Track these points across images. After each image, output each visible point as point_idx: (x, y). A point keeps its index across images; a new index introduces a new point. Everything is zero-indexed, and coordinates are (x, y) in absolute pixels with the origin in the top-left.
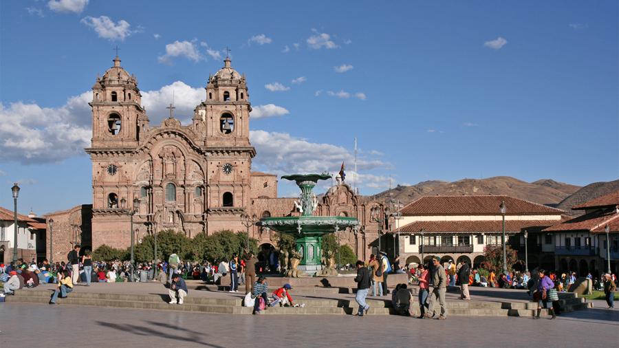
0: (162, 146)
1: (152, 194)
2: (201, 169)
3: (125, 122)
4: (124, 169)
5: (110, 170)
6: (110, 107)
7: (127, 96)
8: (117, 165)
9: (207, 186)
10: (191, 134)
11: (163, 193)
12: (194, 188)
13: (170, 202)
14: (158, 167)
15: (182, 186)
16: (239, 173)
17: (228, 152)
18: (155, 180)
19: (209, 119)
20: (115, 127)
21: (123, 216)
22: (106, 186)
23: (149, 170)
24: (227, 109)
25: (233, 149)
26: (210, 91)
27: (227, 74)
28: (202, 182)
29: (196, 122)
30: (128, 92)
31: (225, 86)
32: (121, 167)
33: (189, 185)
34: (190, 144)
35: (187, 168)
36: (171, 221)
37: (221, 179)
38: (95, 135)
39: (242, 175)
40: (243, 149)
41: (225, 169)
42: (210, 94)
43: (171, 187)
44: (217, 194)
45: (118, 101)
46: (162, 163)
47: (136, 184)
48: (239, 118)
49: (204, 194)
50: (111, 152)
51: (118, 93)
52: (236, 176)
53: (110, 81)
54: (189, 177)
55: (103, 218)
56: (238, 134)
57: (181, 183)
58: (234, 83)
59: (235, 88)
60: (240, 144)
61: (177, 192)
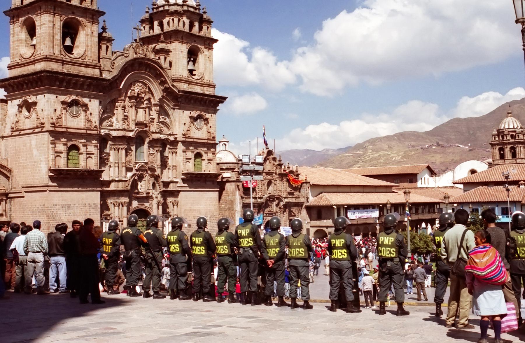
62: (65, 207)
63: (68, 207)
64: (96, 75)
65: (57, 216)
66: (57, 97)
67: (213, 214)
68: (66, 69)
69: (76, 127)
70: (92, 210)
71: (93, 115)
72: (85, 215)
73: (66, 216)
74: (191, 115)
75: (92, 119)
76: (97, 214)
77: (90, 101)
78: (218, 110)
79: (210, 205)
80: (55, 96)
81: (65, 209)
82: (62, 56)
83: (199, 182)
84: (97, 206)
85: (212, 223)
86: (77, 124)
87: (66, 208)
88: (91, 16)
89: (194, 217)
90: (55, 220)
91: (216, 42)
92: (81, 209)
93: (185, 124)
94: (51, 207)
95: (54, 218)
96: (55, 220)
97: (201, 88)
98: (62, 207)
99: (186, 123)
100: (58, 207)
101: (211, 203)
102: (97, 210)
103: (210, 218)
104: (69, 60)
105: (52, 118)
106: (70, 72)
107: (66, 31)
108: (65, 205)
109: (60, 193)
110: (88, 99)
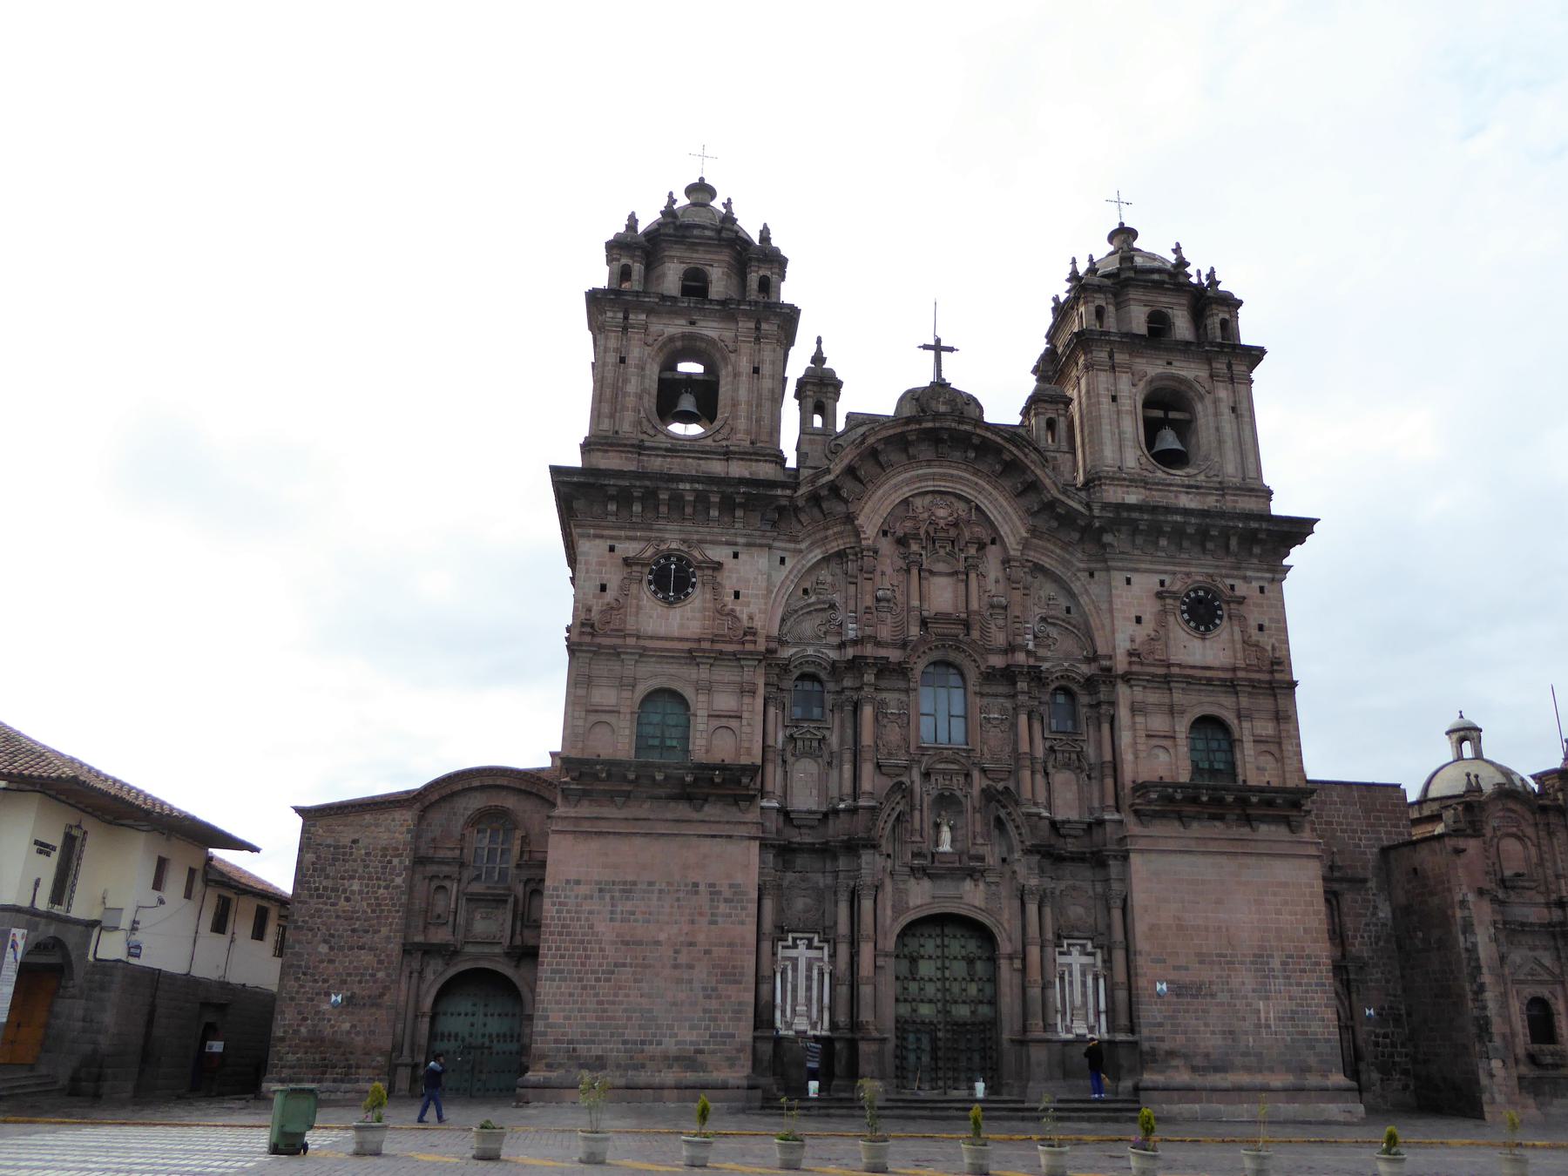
0: (906, 492)
3: (744, 378)
4: (729, 582)
6: (683, 322)
16: (1254, 632)
21: (712, 811)
22: (643, 654)
24: (1173, 370)
32: (718, 566)
36: (946, 847)
38: (606, 425)
39: (1266, 640)
44: (1159, 723)
48: (1226, 411)
50: (677, 501)
52: (1239, 646)
55: (608, 811)
56: (1230, 468)
62: (610, 891)
63: (624, 891)
65: (579, 919)
66: (612, 549)
67: (1303, 949)
70: (723, 908)
72: (693, 922)
73: (612, 920)
75: (738, 609)
76: (743, 923)
77: (736, 556)
78: (1289, 568)
79: (1278, 912)
80: (605, 544)
81: (612, 898)
82: (645, 437)
83: (1218, 824)
84: (745, 893)
85: (1299, 984)
86: (682, 626)
87: (617, 894)
88: (752, 325)
89: (1198, 954)
90: (568, 934)
91: (1260, 359)
92: (678, 899)
93: (1139, 620)
94: (555, 889)
95: (563, 926)
96: (568, 934)
98: (601, 890)
99: (1145, 618)
100: (583, 889)
101: (1286, 903)
102: (743, 908)
103: (1284, 963)
105: (589, 610)
108: (614, 883)
109: (595, 845)
110: (729, 551)
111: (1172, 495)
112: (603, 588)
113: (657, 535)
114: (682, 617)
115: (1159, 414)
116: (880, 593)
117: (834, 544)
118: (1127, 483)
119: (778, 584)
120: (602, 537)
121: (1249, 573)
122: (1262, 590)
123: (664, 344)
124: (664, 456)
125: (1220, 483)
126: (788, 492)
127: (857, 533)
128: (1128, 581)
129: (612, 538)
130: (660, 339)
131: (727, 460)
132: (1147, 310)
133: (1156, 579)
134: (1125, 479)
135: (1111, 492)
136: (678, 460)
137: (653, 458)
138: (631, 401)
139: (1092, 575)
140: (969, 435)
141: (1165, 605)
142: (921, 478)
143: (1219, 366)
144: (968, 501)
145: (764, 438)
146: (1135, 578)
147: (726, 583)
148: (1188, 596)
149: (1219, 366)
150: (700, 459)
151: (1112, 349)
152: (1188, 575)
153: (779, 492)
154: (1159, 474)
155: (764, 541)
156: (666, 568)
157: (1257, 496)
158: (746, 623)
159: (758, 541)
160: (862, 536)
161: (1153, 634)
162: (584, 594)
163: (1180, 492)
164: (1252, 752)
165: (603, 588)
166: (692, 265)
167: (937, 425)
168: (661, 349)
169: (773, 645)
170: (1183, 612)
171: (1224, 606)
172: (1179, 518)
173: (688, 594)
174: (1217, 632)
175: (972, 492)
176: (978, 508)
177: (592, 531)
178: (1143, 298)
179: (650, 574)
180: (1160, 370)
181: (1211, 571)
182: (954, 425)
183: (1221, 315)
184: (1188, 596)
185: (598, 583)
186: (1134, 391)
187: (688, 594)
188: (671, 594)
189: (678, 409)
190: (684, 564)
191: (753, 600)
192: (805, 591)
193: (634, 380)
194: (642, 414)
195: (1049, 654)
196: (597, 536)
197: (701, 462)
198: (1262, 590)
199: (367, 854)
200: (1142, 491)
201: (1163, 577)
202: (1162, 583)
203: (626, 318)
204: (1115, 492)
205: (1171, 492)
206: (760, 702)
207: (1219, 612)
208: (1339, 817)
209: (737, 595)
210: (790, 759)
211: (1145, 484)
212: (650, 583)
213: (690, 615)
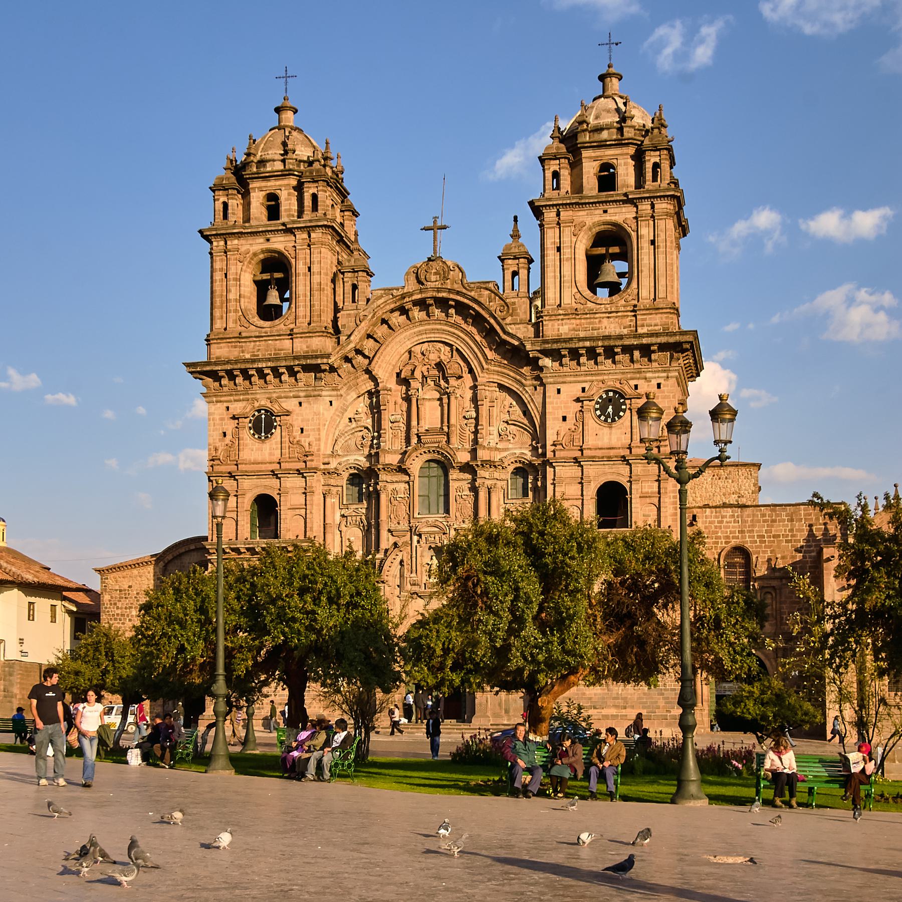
0: (409, 345)
1: (377, 494)
2: (526, 413)
3: (301, 278)
4: (296, 420)
5: (257, 427)
6: (261, 240)
7: (308, 202)
8: (276, 408)
9: (547, 463)
10: (495, 305)
11: (411, 490)
12: (507, 474)
13: (432, 518)
14: (393, 411)
15: (467, 468)
17: (610, 353)
18: (385, 451)
19: (551, 255)
20: (273, 298)
22: (246, 474)
23: (369, 422)
24: (607, 218)
25: (627, 342)
26: (553, 166)
27: (608, 111)
28: (528, 455)
29: (512, 265)
30: (309, 191)
31: (602, 145)
32: (288, 413)
33: (491, 464)
34: (489, 333)
35: (484, 411)
37: (590, 441)
40: (663, 340)
41: (603, 409)
42: (556, 175)
43: (436, 471)
45: (284, 219)
46: (407, 399)
47: (332, 466)
48: (645, 245)
49: (535, 489)
50: (260, 371)
51: (283, 195)
53: (262, 162)
54: (489, 437)
56: (646, 293)
57: (463, 457)
58: (628, 133)
59: (631, 150)
60: (652, 323)
61: (453, 485)
64: (313, 351)
66: (228, 408)
68: (248, 353)
69: (268, 460)
71: (307, 431)
74: (583, 394)
75: (303, 439)
77: (300, 404)
86: (270, 454)
88: (305, 236)
93: (564, 419)
97: (620, 325)
104: (257, 334)
105: (216, 450)
106: (258, 355)
107: (265, 278)
110: (295, 401)
111: (597, 320)
112: (225, 434)
113: (252, 396)
114: (270, 449)
115: (602, 250)
116: (392, 418)
117: (364, 387)
118: (562, 317)
119: (329, 419)
120: (221, 402)
121: (649, 375)
122: (659, 386)
123: (252, 259)
124: (254, 341)
125: (635, 306)
126: (325, 361)
127: (374, 379)
128: (559, 391)
129: (226, 401)
130: (248, 255)
131: (292, 339)
132: (596, 165)
133: (579, 386)
134: (560, 315)
135: (550, 326)
136: (263, 342)
137: (248, 344)
138: (232, 306)
139: (536, 389)
140: (446, 300)
141: (582, 407)
142: (420, 333)
143: (644, 207)
144: (451, 346)
145: (315, 319)
146: (563, 387)
147: (294, 423)
148: (601, 397)
149: (644, 207)
150: (276, 340)
151: (558, 210)
152: (603, 382)
153: (319, 361)
154: (590, 305)
155: (316, 393)
156: (259, 417)
157: (662, 313)
158: (307, 449)
159: (312, 394)
160: (379, 381)
161: (573, 428)
162: (214, 440)
163: (603, 318)
164: (638, 505)
165: (225, 434)
166: (268, 192)
167: (424, 295)
168: (250, 263)
169: (326, 460)
170: (596, 410)
171: (628, 402)
172: (587, 344)
173: (273, 433)
174: (621, 421)
175: (452, 339)
176: (457, 350)
177: (214, 399)
178: (593, 155)
179: (250, 423)
180: (597, 219)
181: (619, 377)
182: (435, 294)
183: (653, 160)
184: (601, 397)
185: (221, 432)
186: (574, 239)
187: (273, 433)
188: (263, 434)
189: (266, 303)
190: (269, 413)
191: (311, 433)
192: (350, 419)
193: (233, 289)
194: (241, 313)
195: (510, 446)
196: (217, 402)
197: (278, 342)
198: (659, 386)
199: (138, 594)
200: (573, 321)
201: (584, 385)
202: (583, 390)
203: (226, 243)
204: (553, 325)
205: (596, 318)
206: (318, 498)
207: (623, 407)
208: (785, 531)
209: (302, 430)
210: (343, 528)
211: (576, 313)
212: (250, 428)
213: (274, 446)
